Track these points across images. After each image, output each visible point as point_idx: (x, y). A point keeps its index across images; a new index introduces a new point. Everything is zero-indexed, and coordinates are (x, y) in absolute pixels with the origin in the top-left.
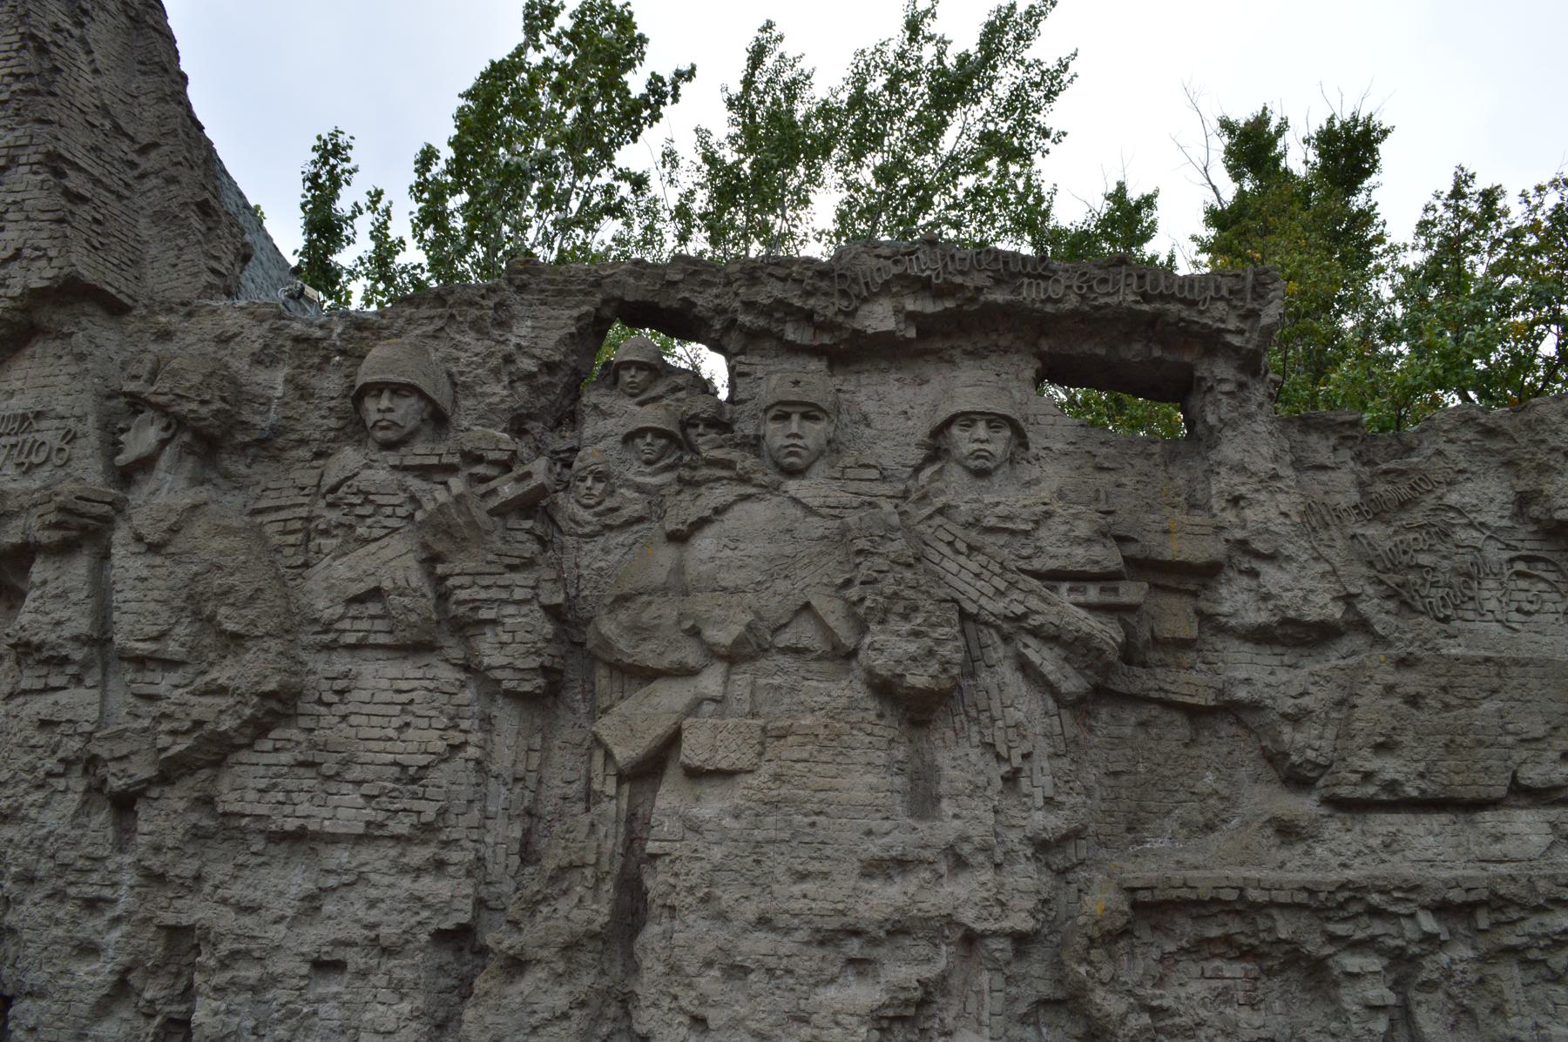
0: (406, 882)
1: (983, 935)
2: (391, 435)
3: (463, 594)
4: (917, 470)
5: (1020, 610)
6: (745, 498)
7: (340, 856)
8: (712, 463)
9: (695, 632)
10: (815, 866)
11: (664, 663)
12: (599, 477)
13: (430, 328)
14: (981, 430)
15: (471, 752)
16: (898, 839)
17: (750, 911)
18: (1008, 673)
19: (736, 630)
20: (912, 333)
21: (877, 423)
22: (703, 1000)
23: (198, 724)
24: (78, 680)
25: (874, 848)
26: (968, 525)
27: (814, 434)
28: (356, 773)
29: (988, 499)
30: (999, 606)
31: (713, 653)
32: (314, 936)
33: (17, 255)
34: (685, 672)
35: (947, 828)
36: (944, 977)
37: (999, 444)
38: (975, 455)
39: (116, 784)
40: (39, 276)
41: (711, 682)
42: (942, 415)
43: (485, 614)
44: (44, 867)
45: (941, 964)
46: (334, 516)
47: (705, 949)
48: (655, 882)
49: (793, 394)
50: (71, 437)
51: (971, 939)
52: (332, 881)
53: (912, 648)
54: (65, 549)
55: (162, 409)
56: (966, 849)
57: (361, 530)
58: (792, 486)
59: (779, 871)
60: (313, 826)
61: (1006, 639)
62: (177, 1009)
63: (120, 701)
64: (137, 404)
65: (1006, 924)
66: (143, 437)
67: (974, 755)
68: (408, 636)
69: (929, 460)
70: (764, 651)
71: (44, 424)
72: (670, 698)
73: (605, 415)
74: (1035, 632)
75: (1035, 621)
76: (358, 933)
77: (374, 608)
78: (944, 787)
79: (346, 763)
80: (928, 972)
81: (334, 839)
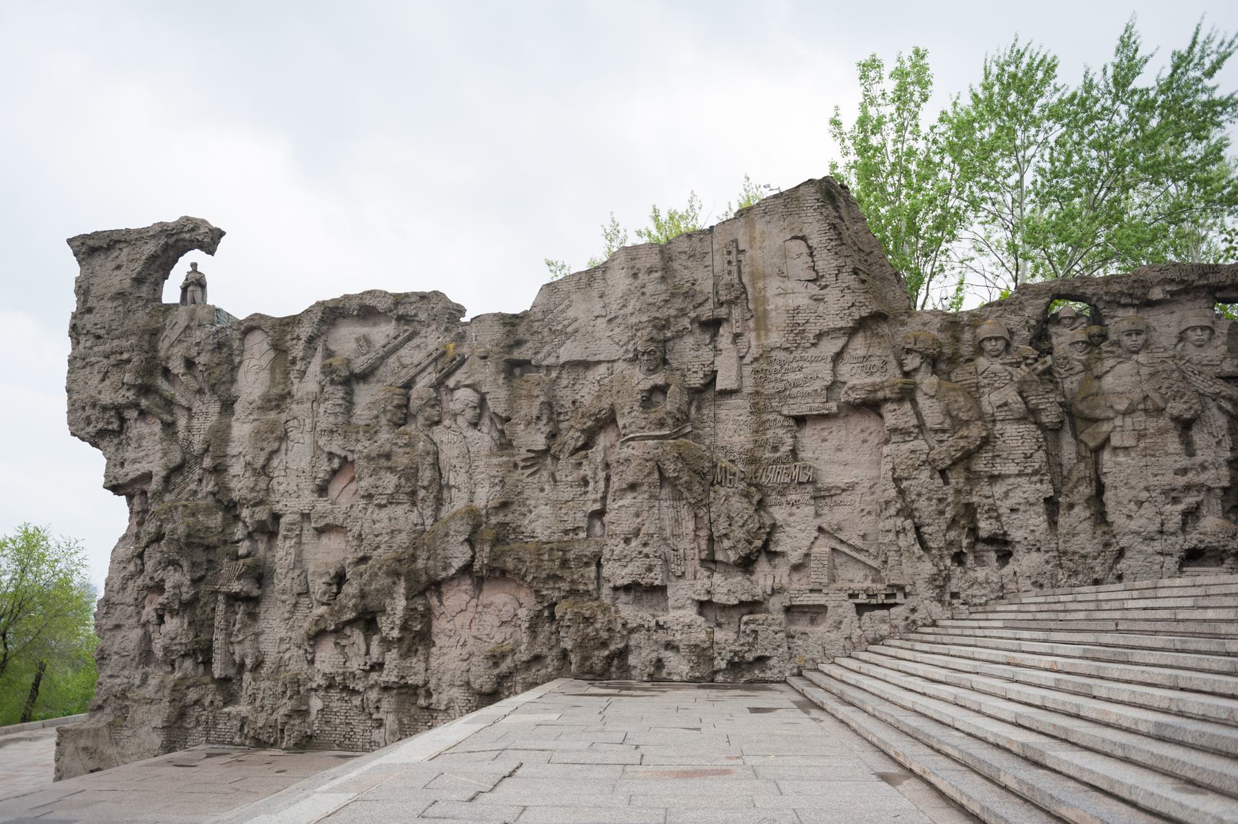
0: (1033, 486)
1: (1214, 488)
2: (996, 353)
3: (1034, 402)
4: (1176, 345)
5: (1218, 391)
6: (1119, 363)
7: (1011, 480)
8: (1106, 352)
9: (1111, 407)
10: (1160, 472)
11: (1103, 416)
12: (1064, 359)
13: (998, 314)
14: (1199, 332)
15: (1044, 448)
16: (1184, 462)
17: (1142, 485)
18: (1215, 411)
19: (1126, 406)
20: (1169, 297)
21: (1158, 329)
22: (1130, 510)
23: (963, 447)
24: (916, 438)
25: (1178, 466)
26: (1197, 364)
27: (1140, 339)
28: (1011, 457)
29: (1203, 355)
30: (1211, 390)
31: (1118, 412)
32: (1010, 503)
33: (853, 305)
34: (1108, 419)
35: (1199, 458)
36: (1202, 501)
37: (1205, 336)
38: (1197, 340)
39: (939, 468)
40: (864, 312)
41: (1118, 422)
42: (1184, 327)
43: (1041, 407)
44: (924, 491)
45: (1202, 497)
46: (986, 381)
47: (1130, 497)
48: (1107, 481)
49: (1133, 328)
50: (885, 363)
51: (1209, 489)
52: (1011, 487)
53: (1185, 406)
54: (900, 400)
55: (921, 353)
56: (1206, 464)
57: (996, 385)
58: (1135, 357)
59: (1149, 474)
60: (1003, 472)
61: (1214, 400)
62: (971, 526)
63: (933, 443)
64: (909, 351)
65: (1221, 485)
66: (912, 362)
67: (1206, 436)
68: (1017, 416)
69: (1179, 342)
70: (1133, 411)
71: (872, 359)
72: (1106, 427)
73: (1060, 336)
74: (1223, 397)
75: (1223, 394)
76: (1022, 501)
77: (1006, 408)
78: (1197, 447)
79: (1009, 454)
80: (1198, 499)
81: (1009, 476)
